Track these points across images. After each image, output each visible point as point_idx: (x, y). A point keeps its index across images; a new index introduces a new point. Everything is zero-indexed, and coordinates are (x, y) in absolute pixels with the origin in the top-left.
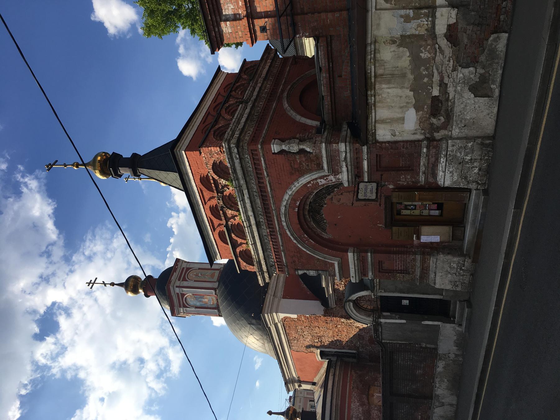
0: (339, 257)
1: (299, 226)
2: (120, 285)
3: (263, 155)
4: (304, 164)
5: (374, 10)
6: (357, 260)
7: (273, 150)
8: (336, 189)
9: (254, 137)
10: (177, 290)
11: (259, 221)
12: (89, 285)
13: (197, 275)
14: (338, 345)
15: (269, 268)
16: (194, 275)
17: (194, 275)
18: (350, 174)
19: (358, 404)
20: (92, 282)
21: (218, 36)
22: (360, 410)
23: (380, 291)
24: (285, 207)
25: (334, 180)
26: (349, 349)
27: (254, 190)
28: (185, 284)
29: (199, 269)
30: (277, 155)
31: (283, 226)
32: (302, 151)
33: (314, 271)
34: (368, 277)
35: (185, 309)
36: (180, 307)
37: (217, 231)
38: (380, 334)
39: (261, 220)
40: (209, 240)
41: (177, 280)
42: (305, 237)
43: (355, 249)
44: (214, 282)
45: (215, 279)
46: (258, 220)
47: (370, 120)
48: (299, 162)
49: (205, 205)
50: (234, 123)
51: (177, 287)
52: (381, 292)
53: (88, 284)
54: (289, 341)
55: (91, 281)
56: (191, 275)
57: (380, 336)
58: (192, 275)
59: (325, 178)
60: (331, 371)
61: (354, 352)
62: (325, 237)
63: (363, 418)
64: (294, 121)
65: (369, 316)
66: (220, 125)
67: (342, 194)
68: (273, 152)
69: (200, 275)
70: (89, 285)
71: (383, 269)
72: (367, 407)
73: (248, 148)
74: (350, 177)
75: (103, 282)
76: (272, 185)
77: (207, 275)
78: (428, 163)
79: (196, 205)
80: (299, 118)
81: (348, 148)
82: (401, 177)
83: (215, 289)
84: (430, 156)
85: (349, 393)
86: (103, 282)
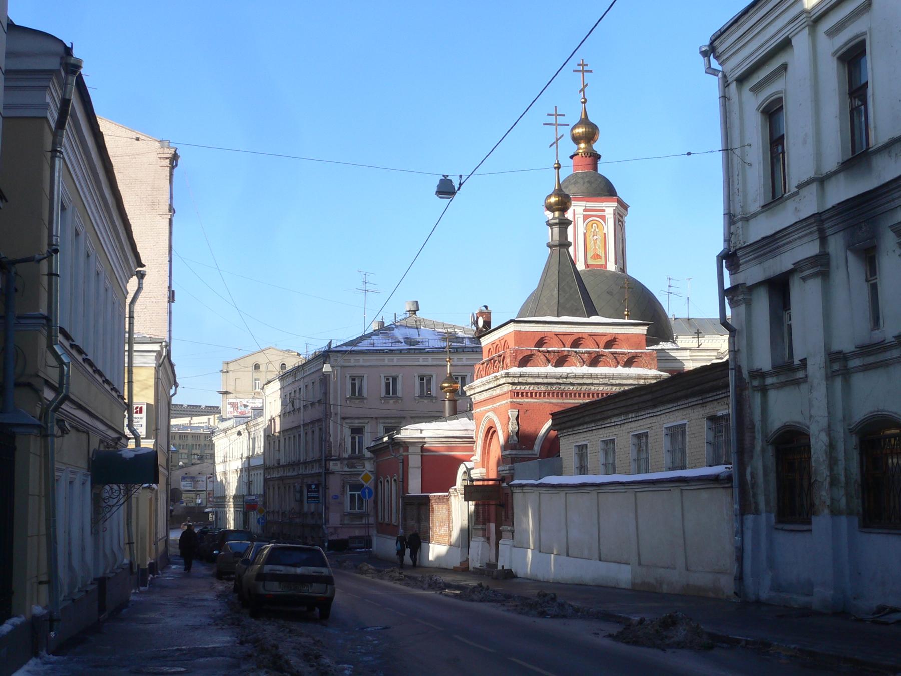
12: (579, 65)
17: (595, 230)
20: (586, 68)
41: (584, 208)
43: (484, 474)
55: (586, 65)
56: (594, 225)
58: (595, 227)
69: (595, 238)
70: (579, 65)
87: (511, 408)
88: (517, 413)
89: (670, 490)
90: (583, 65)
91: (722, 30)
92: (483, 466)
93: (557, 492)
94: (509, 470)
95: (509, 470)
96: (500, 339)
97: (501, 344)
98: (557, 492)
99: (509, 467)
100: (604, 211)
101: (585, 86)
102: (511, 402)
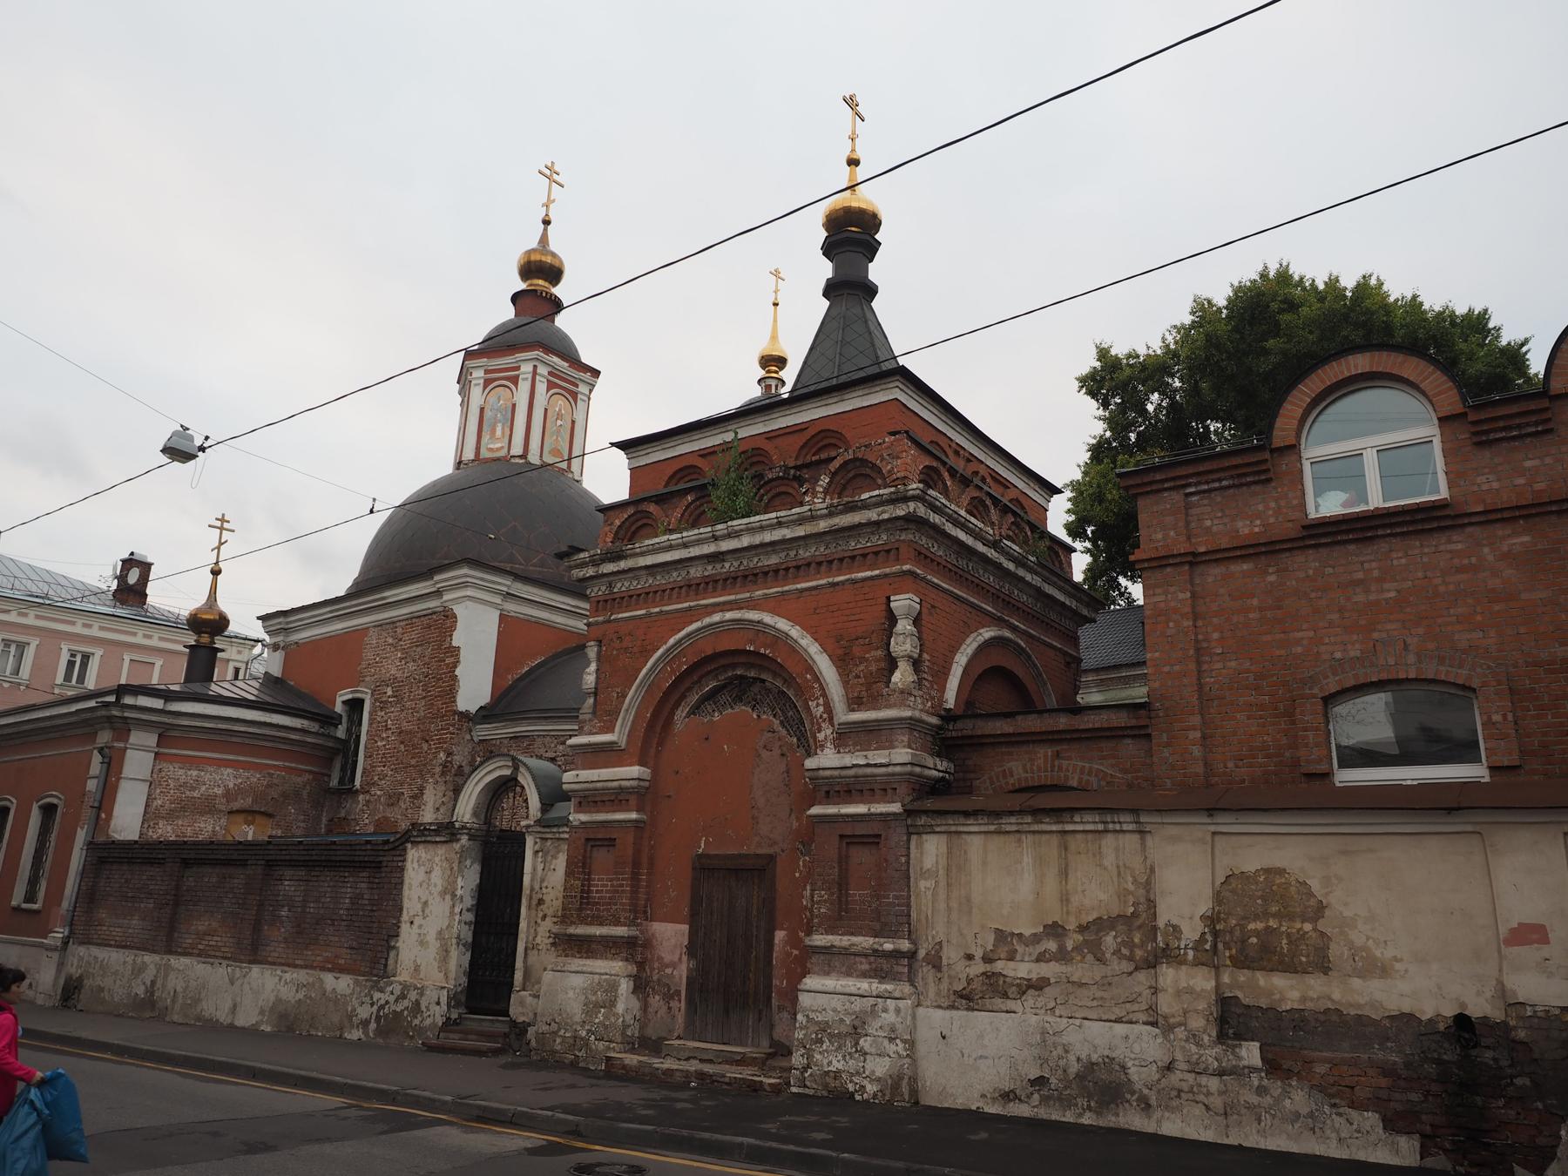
0: (628, 742)
1: (709, 652)
2: (544, 240)
3: (886, 575)
4: (862, 668)
5: (1213, 828)
6: (621, 788)
7: (897, 597)
8: (795, 740)
10: (527, 368)
11: (724, 561)
13: (559, 416)
14: (376, 742)
15: (606, 579)
16: (560, 410)
17: (560, 410)
18: (836, 773)
19: (231, 786)
20: (555, 176)
21: (1154, 487)
22: (216, 790)
23: (538, 840)
24: (758, 622)
25: (821, 736)
26: (364, 769)
27: (801, 552)
28: (541, 387)
29: (573, 422)
30: (884, 607)
31: (710, 614)
32: (892, 664)
33: (593, 685)
34: (577, 812)
35: (482, 381)
36: (487, 372)
37: (699, 462)
38: (429, 839)
39: (727, 565)
40: (680, 442)
42: (680, 666)
43: (647, 784)
44: (541, 456)
46: (728, 557)
47: (962, 820)
48: (867, 656)
49: (767, 438)
50: (956, 512)
51: (535, 367)
52: (536, 843)
54: (393, 623)
57: (423, 839)
59: (825, 716)
60: (313, 724)
61: (357, 783)
62: (678, 712)
64: (954, 650)
65: (475, 814)
67: (783, 755)
68: (892, 598)
69: (559, 422)
71: (595, 849)
72: (223, 808)
73: (904, 541)
74: (828, 773)
75: (554, 201)
76: (813, 593)
78: (855, 955)
79: (766, 418)
80: (961, 660)
81: (898, 769)
82: (823, 892)
83: (524, 456)
84: (872, 959)
86: (554, 201)
98: (1469, 828)
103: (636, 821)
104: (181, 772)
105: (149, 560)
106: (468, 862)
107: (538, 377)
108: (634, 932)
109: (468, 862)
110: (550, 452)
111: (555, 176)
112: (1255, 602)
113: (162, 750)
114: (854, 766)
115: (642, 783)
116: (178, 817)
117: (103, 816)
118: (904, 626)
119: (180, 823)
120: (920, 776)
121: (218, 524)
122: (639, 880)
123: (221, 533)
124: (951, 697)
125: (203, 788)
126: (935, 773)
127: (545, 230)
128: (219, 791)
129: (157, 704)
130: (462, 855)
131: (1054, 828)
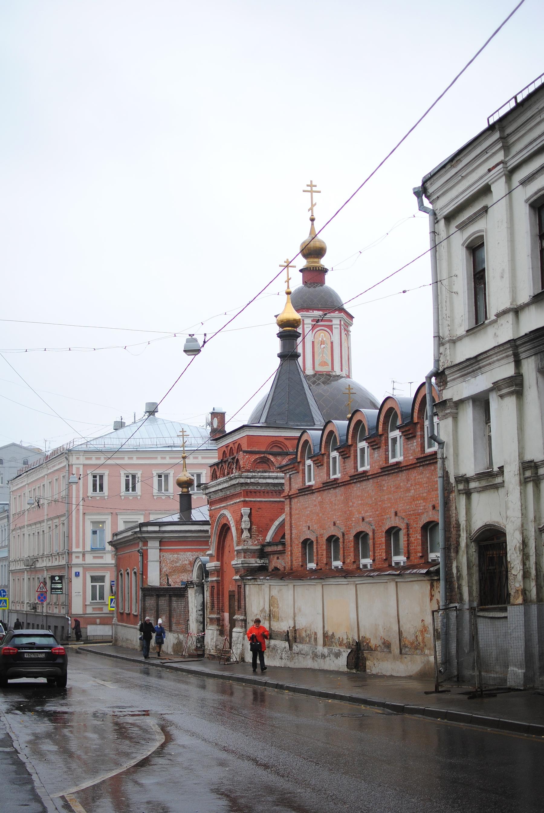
9: (255, 492)
12: (308, 186)
13: (322, 343)
16: (322, 339)
17: (322, 339)
19: (191, 559)
20: (314, 189)
22: (185, 562)
29: (332, 343)
32: (242, 532)
41: (312, 319)
43: (219, 568)
44: (314, 368)
45: (318, 368)
53: (309, 184)
55: (315, 186)
63: (178, 565)
65: (197, 578)
66: (272, 460)
69: (323, 346)
70: (308, 186)
75: (315, 204)
77: (324, 355)
85: (203, 549)
87: (244, 507)
88: (249, 511)
89: (387, 582)
90: (311, 185)
91: (432, 174)
92: (218, 560)
93: (287, 584)
94: (242, 564)
95: (242, 564)
96: (234, 443)
97: (234, 447)
99: (242, 561)
100: (331, 321)
101: (313, 205)
102: (244, 501)
103: (216, 580)
104: (171, 556)
105: (223, 411)
106: (197, 594)
107: (305, 326)
108: (218, 616)
109: (197, 594)
110: (319, 365)
111: (314, 189)
112: (297, 511)
113: (162, 548)
114: (236, 564)
115: (216, 568)
116: (173, 575)
117: (144, 577)
118: (246, 518)
119: (174, 577)
120: (248, 566)
121: (181, 434)
122: (220, 599)
123: (183, 438)
124: (268, 539)
125: (180, 562)
126: (258, 565)
127: (313, 224)
128: (187, 562)
129: (156, 528)
130: (196, 592)
131: (256, 583)
